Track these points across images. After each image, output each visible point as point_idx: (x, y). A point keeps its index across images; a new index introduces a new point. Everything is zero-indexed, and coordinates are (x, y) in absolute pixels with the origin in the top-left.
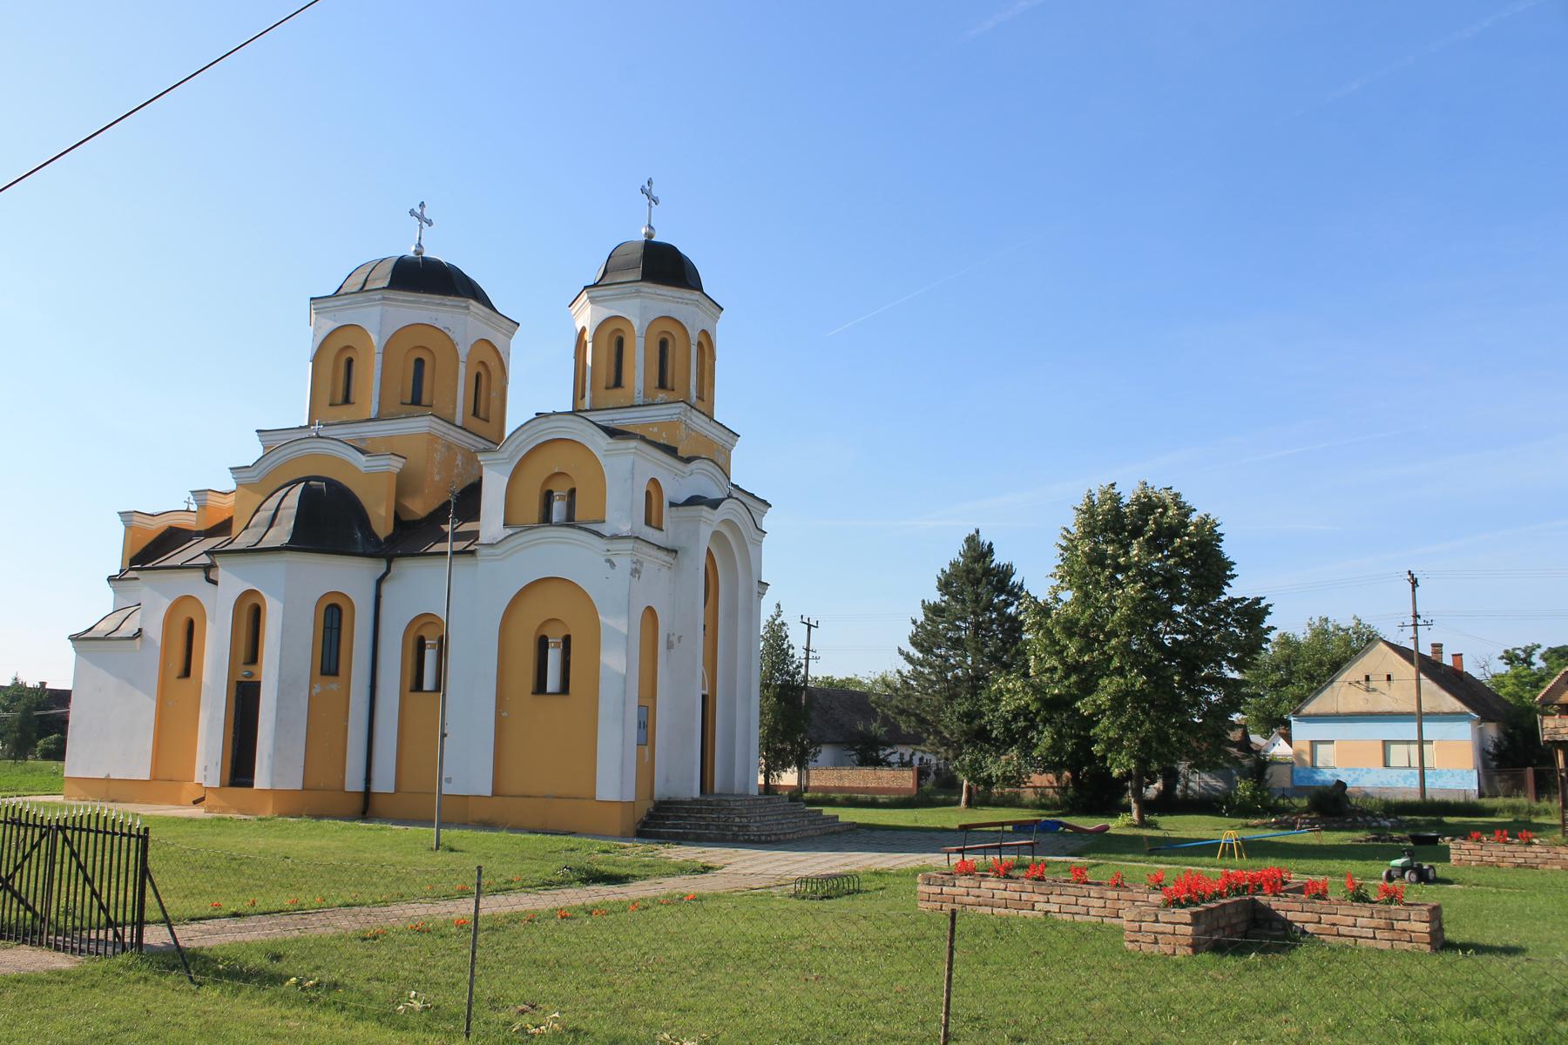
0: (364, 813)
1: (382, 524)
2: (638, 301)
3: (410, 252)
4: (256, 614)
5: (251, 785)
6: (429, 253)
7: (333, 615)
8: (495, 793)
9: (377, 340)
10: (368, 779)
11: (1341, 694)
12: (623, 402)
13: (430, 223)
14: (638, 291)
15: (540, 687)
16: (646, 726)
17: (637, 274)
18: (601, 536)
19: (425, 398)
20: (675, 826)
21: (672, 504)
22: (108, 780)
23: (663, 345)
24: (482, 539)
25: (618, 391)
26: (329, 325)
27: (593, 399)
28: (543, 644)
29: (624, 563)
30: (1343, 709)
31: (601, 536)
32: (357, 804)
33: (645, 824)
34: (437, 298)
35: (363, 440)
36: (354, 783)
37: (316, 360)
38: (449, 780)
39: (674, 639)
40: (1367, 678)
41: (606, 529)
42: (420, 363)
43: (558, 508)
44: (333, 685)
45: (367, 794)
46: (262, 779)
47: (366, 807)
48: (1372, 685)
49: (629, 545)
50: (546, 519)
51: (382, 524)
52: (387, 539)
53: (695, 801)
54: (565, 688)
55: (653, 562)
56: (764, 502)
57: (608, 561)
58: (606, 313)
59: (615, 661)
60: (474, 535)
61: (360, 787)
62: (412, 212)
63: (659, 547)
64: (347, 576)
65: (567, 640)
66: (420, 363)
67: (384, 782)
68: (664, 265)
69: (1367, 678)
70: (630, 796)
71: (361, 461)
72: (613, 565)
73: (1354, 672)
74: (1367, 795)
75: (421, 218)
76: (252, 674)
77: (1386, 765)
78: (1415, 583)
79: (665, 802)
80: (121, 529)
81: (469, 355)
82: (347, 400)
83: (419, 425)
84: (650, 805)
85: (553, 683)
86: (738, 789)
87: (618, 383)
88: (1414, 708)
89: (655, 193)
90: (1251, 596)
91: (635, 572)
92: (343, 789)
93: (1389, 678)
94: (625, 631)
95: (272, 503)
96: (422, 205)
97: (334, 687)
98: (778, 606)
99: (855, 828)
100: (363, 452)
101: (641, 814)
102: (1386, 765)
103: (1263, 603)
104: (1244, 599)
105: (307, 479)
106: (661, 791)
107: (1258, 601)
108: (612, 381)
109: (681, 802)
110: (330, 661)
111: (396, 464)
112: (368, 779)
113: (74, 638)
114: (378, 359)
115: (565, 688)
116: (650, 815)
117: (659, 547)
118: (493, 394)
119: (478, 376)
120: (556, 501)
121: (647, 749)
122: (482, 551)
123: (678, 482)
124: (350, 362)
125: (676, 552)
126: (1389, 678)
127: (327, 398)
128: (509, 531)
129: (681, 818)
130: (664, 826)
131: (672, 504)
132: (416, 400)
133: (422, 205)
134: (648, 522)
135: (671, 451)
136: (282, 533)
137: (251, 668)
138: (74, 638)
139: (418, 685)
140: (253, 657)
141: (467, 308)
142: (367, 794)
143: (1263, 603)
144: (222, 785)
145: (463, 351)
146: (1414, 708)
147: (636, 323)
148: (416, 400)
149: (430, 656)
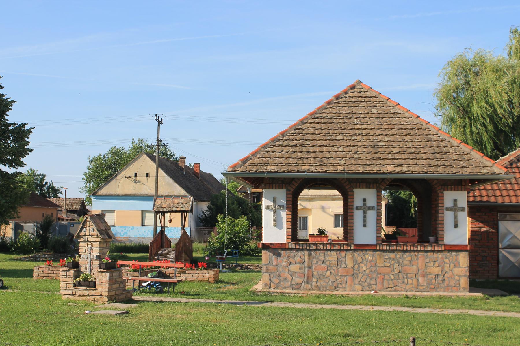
11: (121, 184)
30: (121, 192)
40: (136, 175)
48: (138, 179)
69: (136, 175)
73: (129, 171)
74: (131, 241)
77: (143, 225)
78: (160, 122)
88: (153, 192)
90: (19, 123)
93: (147, 175)
102: (143, 225)
103: (27, 128)
104: (14, 124)
107: (23, 125)
126: (147, 175)
143: (27, 128)
146: (153, 192)
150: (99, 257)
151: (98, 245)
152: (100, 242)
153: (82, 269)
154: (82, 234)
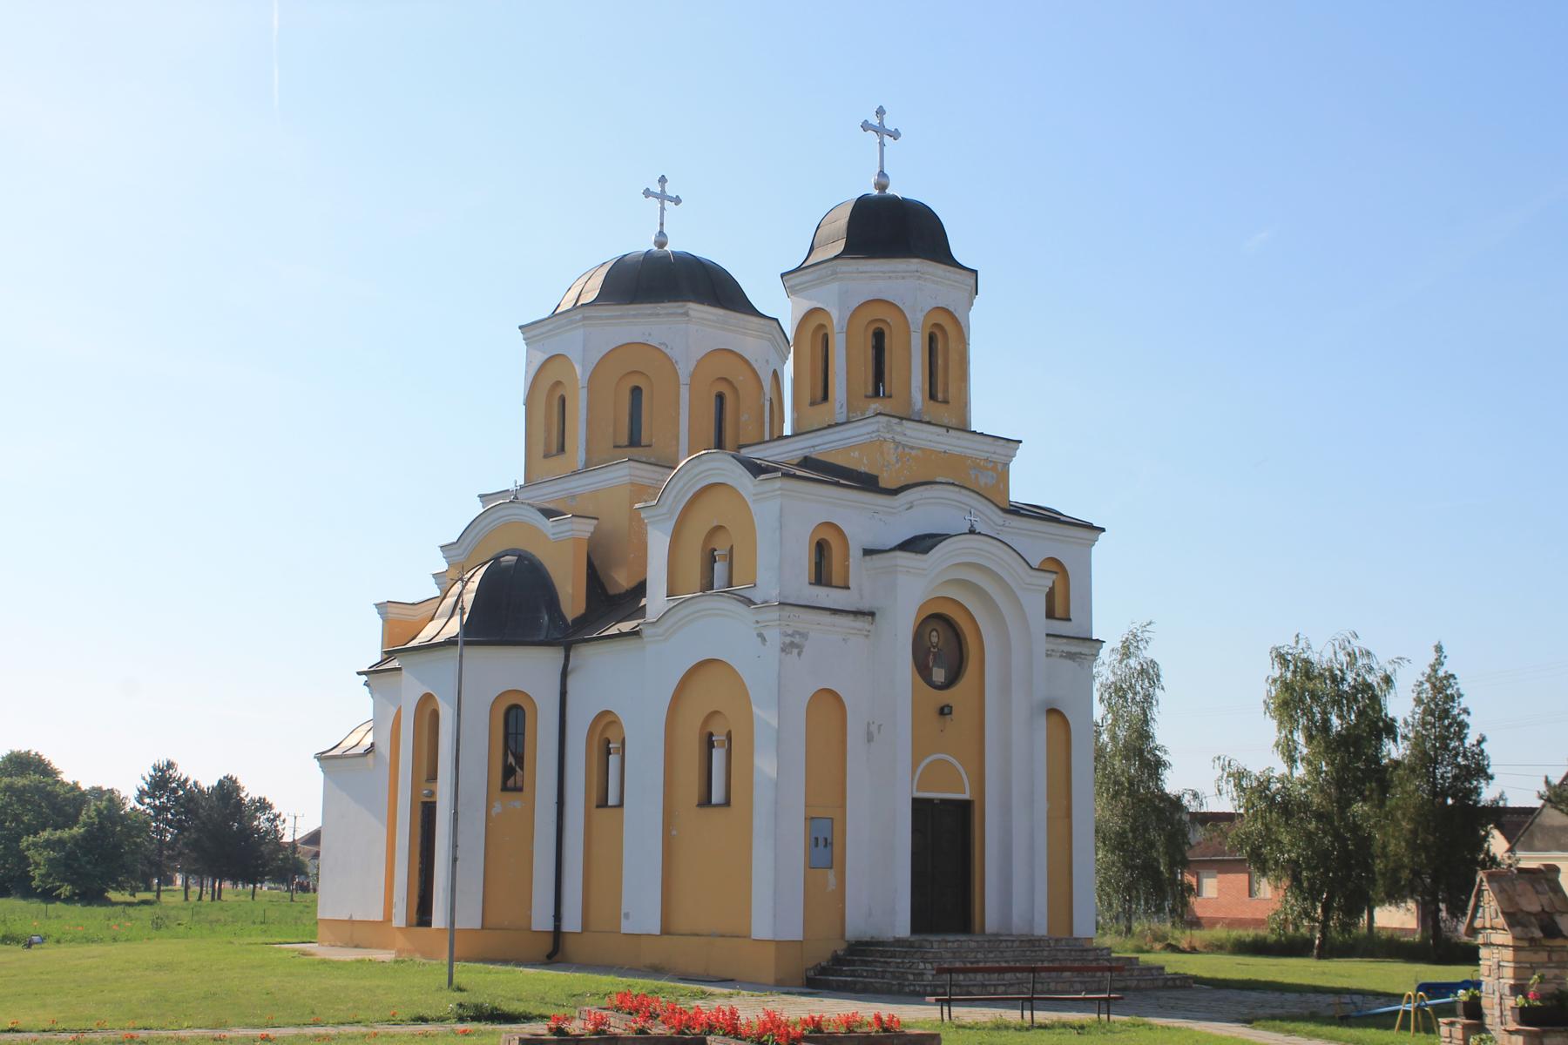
0: (549, 957)
1: (572, 597)
2: (835, 286)
3: (643, 244)
4: (435, 715)
5: (428, 923)
6: (677, 244)
7: (513, 720)
8: (666, 931)
9: (581, 372)
10: (558, 917)
12: (828, 421)
13: (677, 201)
14: (834, 273)
15: (706, 801)
16: (824, 844)
17: (840, 246)
18: (749, 602)
19: (644, 441)
20: (853, 974)
21: (868, 552)
22: (351, 922)
23: (879, 336)
24: (651, 616)
25: (824, 407)
26: (540, 357)
27: (796, 422)
28: (710, 744)
29: (774, 637)
31: (749, 602)
32: (547, 945)
33: (823, 970)
34: (646, 308)
35: (573, 497)
36: (542, 920)
37: (529, 402)
38: (627, 916)
39: (874, 728)
41: (757, 596)
42: (636, 392)
43: (720, 568)
44: (515, 802)
45: (557, 933)
46: (439, 918)
47: (555, 951)
49: (774, 614)
50: (708, 585)
51: (572, 597)
52: (575, 621)
53: (899, 942)
54: (727, 803)
55: (824, 633)
56: (1089, 527)
57: (760, 635)
58: (807, 305)
59: (772, 767)
60: (641, 612)
61: (550, 927)
62: (647, 193)
63: (835, 611)
64: (526, 670)
65: (729, 736)
66: (636, 392)
67: (571, 923)
68: (891, 228)
70: (796, 933)
71: (547, 525)
72: (764, 640)
75: (662, 197)
76: (432, 793)
79: (867, 944)
80: (380, 621)
81: (693, 376)
82: (562, 449)
83: (621, 474)
84: (840, 948)
85: (717, 795)
86: (1018, 925)
87: (825, 397)
89: (889, 125)
91: (785, 649)
92: (529, 929)
94: (774, 723)
95: (458, 586)
96: (663, 180)
97: (518, 805)
98: (1439, 649)
99: (1185, 983)
100: (548, 513)
101: (823, 952)
105: (497, 559)
106: (858, 925)
108: (819, 393)
109: (882, 943)
110: (511, 770)
111: (585, 529)
112: (558, 917)
113: (322, 758)
114: (583, 395)
115: (727, 803)
116: (837, 960)
117: (835, 611)
118: (744, 417)
119: (720, 398)
120: (713, 566)
121: (831, 875)
122: (647, 631)
123: (864, 521)
124: (563, 400)
125: (872, 614)
127: (539, 449)
128: (672, 604)
129: (865, 963)
130: (841, 973)
131: (868, 552)
132: (634, 441)
133: (663, 180)
134: (821, 576)
135: (867, 483)
136: (454, 628)
137: (430, 786)
138: (322, 758)
139: (603, 803)
140: (433, 777)
141: (686, 314)
142: (557, 933)
144: (409, 925)
145: (684, 371)
147: (835, 314)
148: (634, 441)
149: (614, 760)
150: (1517, 989)
151: (1508, 954)
152: (1516, 949)
153: (1488, 1020)
154: (1478, 923)
